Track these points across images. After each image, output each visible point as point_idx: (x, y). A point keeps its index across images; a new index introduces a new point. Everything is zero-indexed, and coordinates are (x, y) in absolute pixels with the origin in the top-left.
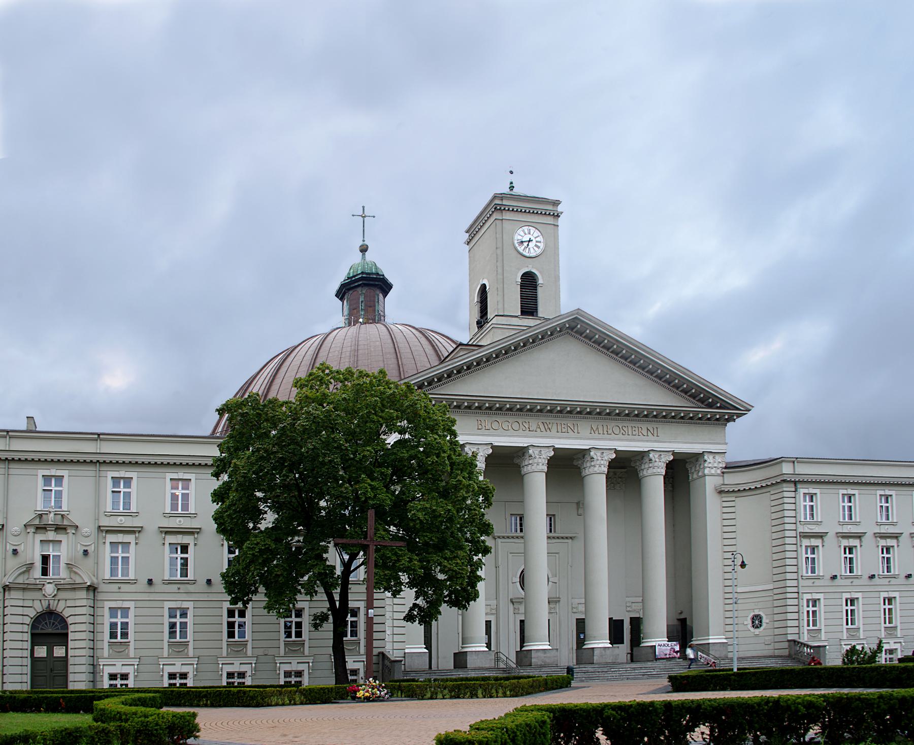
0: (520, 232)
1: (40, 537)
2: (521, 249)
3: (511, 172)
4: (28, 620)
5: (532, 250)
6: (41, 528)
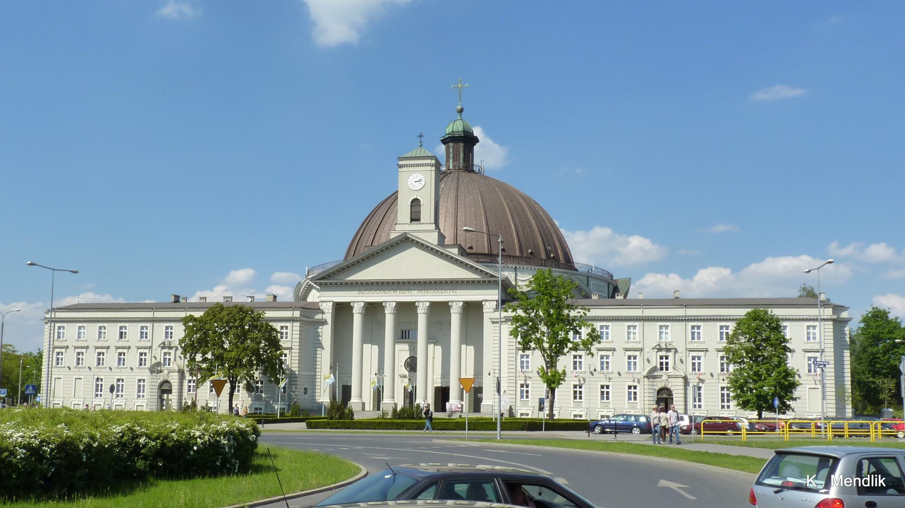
0: (411, 177)
1: (164, 351)
2: (411, 187)
4: (158, 384)
5: (417, 186)
6: (163, 348)
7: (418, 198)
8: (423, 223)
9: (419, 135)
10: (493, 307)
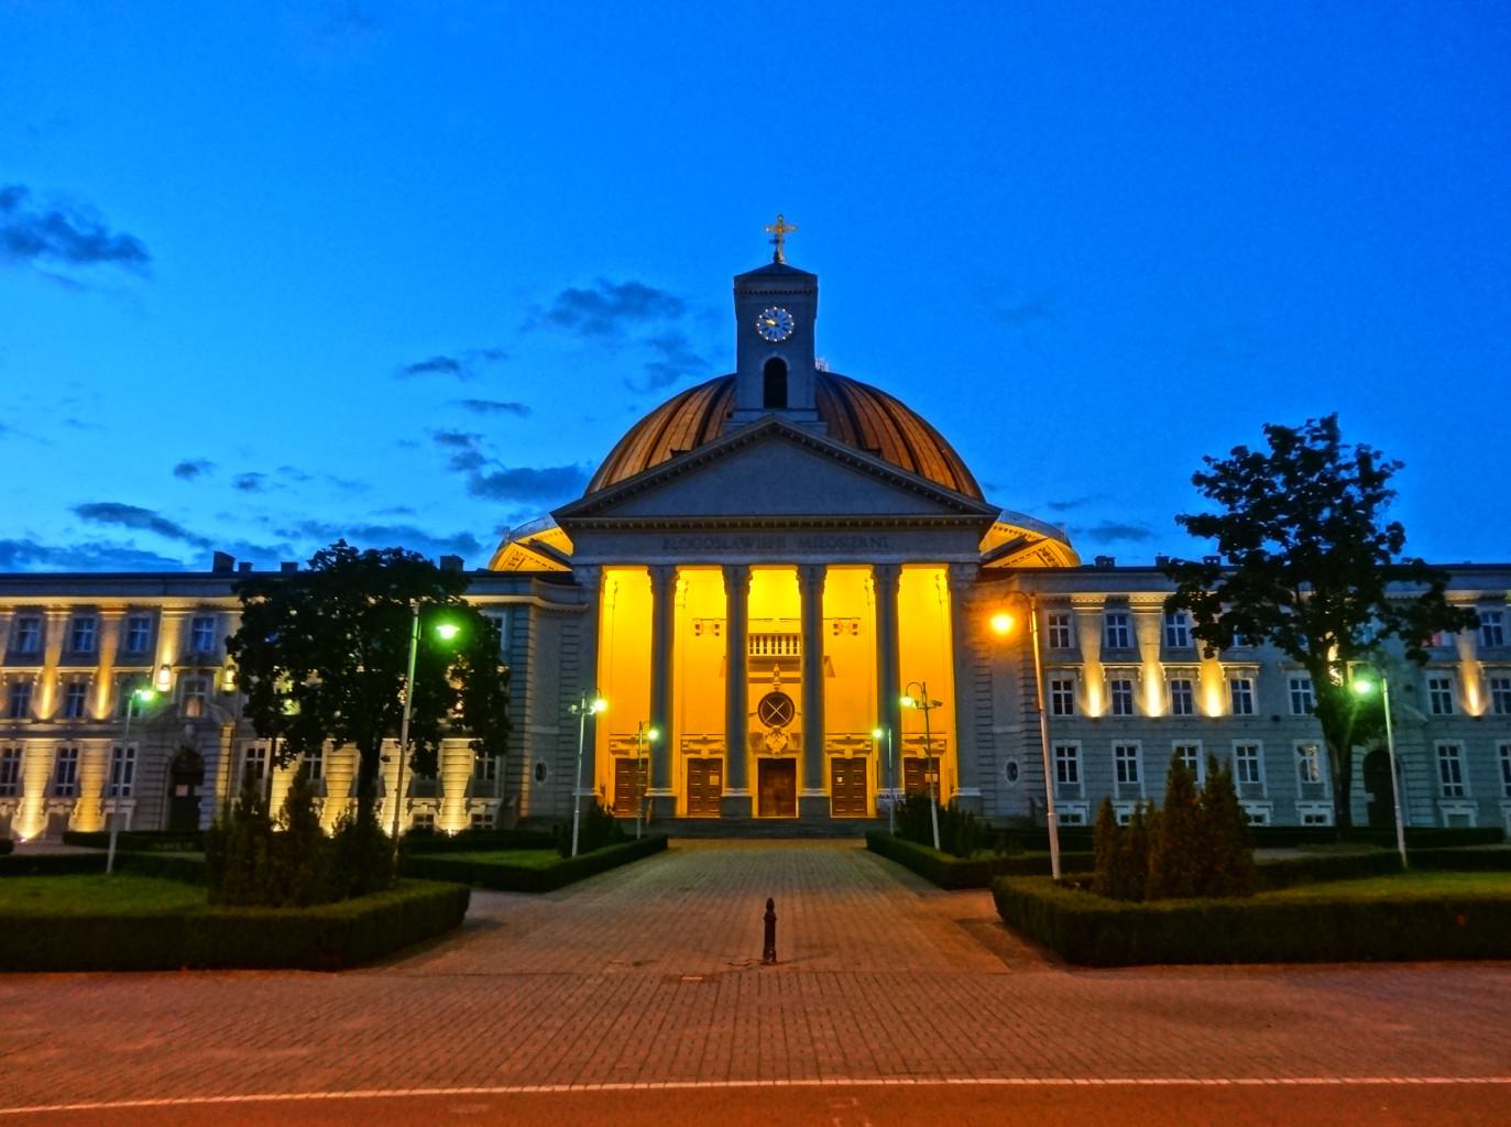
3: (776, 242)
7: (783, 358)
8: (792, 410)
9: (773, 238)
10: (970, 578)
